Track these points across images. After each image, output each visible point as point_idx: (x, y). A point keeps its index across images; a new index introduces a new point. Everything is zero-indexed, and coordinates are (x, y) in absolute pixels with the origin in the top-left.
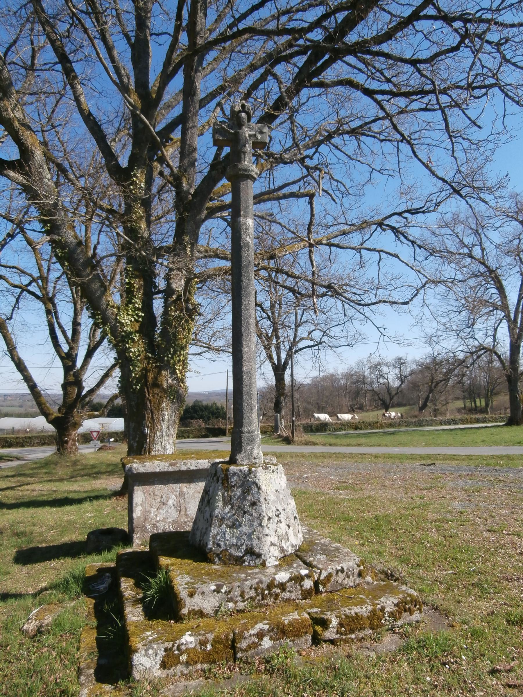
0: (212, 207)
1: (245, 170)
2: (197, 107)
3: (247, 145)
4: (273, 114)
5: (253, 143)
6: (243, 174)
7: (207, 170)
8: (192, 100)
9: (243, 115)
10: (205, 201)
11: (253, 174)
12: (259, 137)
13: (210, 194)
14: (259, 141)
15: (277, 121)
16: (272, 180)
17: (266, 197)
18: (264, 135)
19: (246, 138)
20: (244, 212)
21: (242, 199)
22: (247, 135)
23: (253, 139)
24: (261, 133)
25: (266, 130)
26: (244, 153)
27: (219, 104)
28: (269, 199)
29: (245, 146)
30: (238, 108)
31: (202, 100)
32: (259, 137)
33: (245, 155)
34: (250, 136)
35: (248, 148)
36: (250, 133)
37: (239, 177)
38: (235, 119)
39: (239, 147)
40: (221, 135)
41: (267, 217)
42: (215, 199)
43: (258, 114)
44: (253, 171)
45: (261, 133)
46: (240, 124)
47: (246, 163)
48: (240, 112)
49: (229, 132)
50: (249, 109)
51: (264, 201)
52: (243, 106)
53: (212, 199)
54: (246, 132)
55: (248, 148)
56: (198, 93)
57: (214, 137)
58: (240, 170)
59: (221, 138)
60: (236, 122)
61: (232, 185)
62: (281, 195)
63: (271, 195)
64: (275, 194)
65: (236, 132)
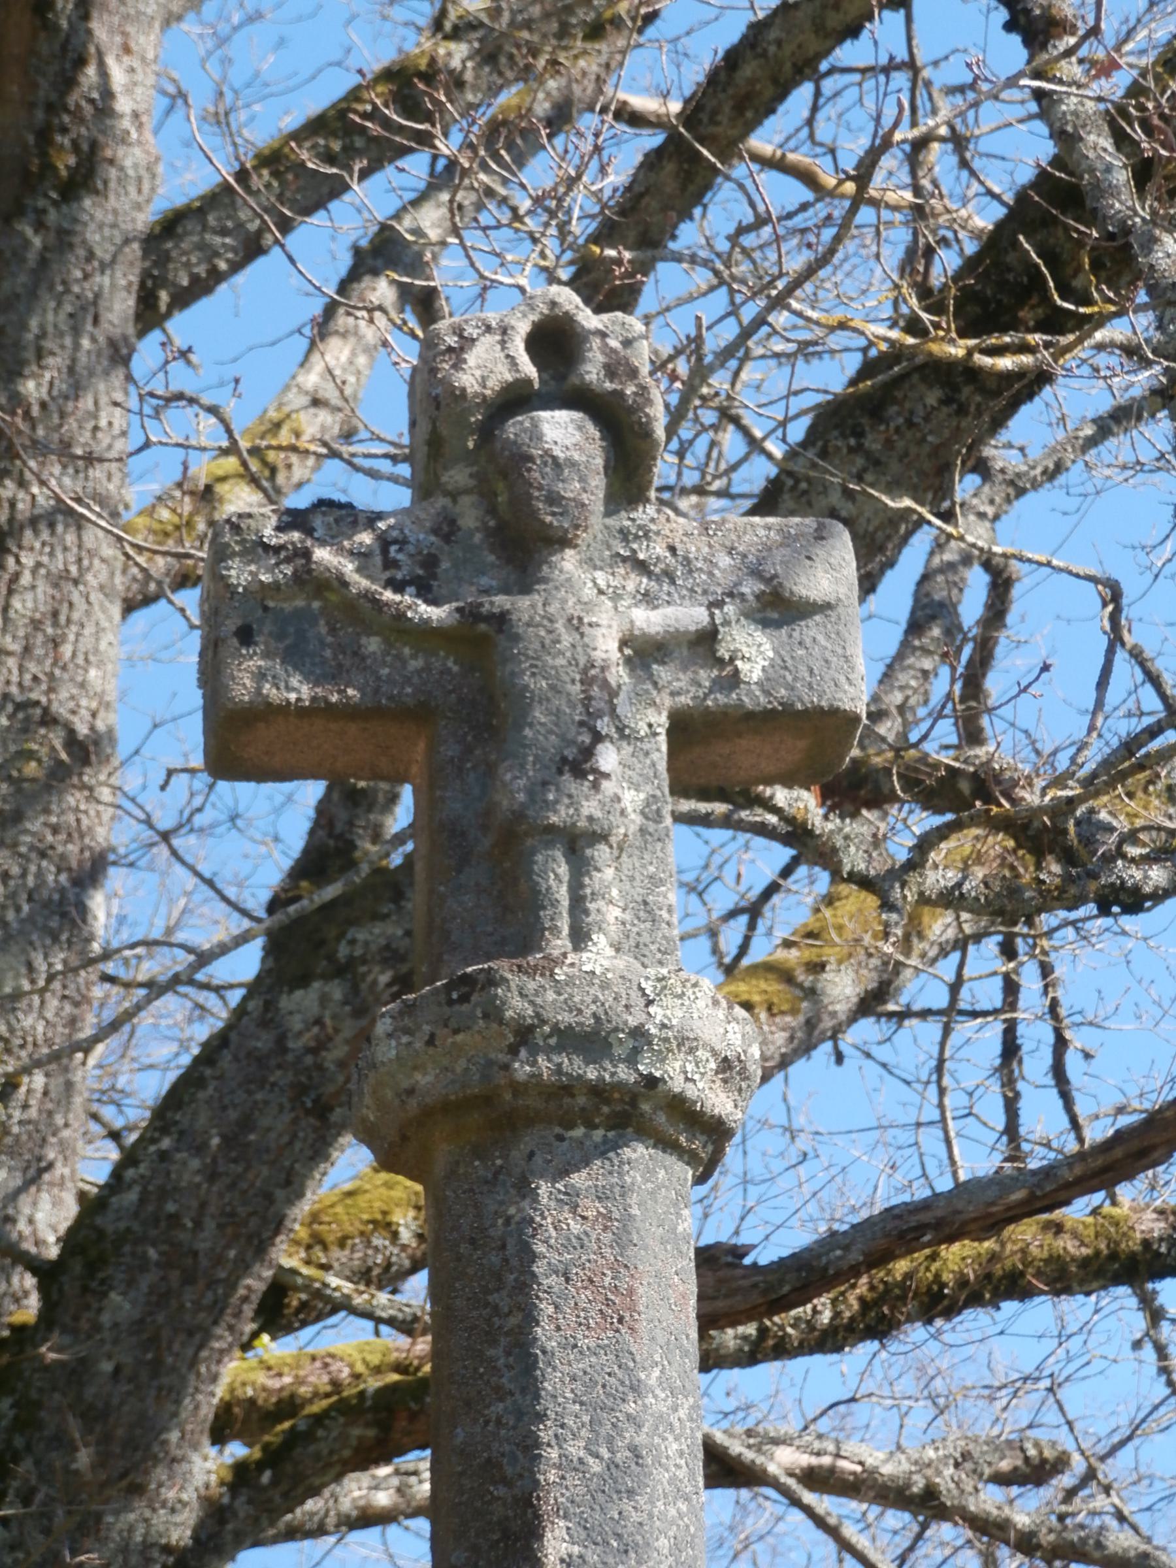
0: (288, 1405)
1: (592, 1041)
2: (120, 307)
3: (608, 758)
4: (968, 372)
5: (685, 730)
6: (566, 1088)
7: (246, 964)
8: (64, 240)
9: (561, 430)
10: (200, 1335)
11: (691, 1078)
12: (754, 651)
13: (260, 1248)
14: (751, 698)
15: (1027, 433)
16: (1036, 1037)
17: (958, 1257)
18: (811, 629)
19: (591, 676)
20: (589, 1533)
21: (555, 1382)
22: (606, 646)
23: (681, 686)
24: (779, 608)
25: (830, 572)
26: (578, 844)
27: (383, 251)
28: (1004, 1285)
29: (580, 764)
30: (491, 364)
31: (172, 225)
32: (754, 651)
33: (580, 866)
34: (644, 652)
35: (627, 781)
36: (650, 620)
37: (522, 1121)
38: (458, 476)
39: (515, 785)
40: (295, 655)
41: (989, 1500)
42: (321, 1307)
43: (779, 397)
44: (686, 1043)
45: (779, 608)
46: (524, 541)
47: (600, 956)
48: (516, 399)
49: (400, 627)
50: (618, 367)
51: (938, 1304)
52: (554, 341)
53: (281, 1310)
54: (593, 610)
55: (627, 781)
56: (131, 158)
57: (211, 674)
58: (524, 1036)
59: (299, 690)
60: (470, 516)
61: (439, 1211)
62: (1150, 1226)
63: (1026, 1234)
64: (1077, 1211)
65: (470, 615)
